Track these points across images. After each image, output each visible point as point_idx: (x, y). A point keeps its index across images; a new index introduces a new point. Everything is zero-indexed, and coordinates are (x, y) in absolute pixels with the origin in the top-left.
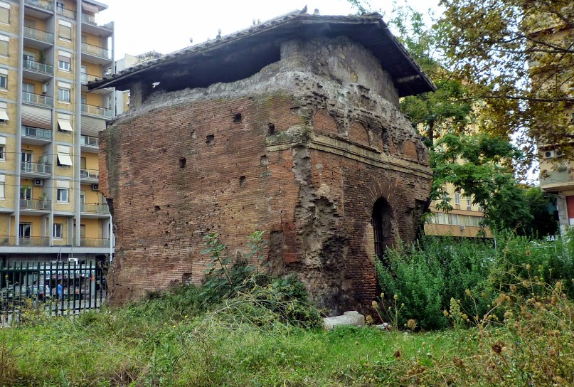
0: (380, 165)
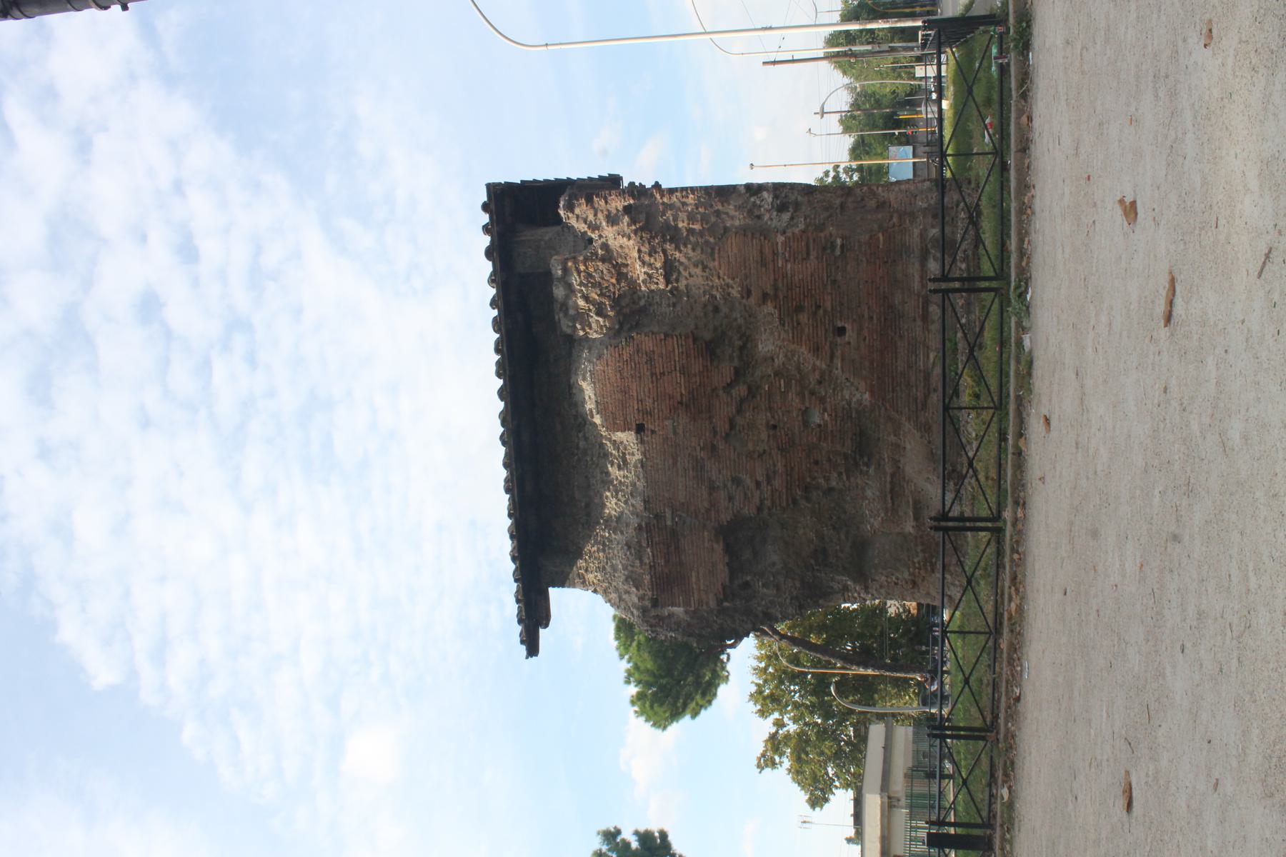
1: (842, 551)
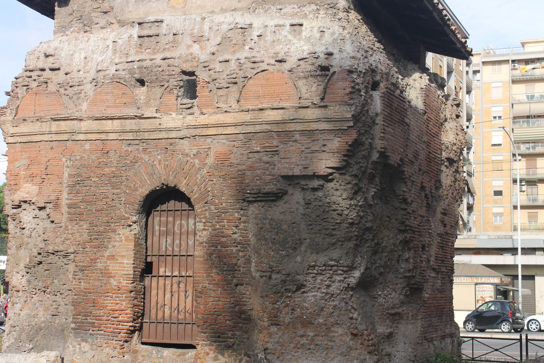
0: (163, 135)
1: (375, 269)
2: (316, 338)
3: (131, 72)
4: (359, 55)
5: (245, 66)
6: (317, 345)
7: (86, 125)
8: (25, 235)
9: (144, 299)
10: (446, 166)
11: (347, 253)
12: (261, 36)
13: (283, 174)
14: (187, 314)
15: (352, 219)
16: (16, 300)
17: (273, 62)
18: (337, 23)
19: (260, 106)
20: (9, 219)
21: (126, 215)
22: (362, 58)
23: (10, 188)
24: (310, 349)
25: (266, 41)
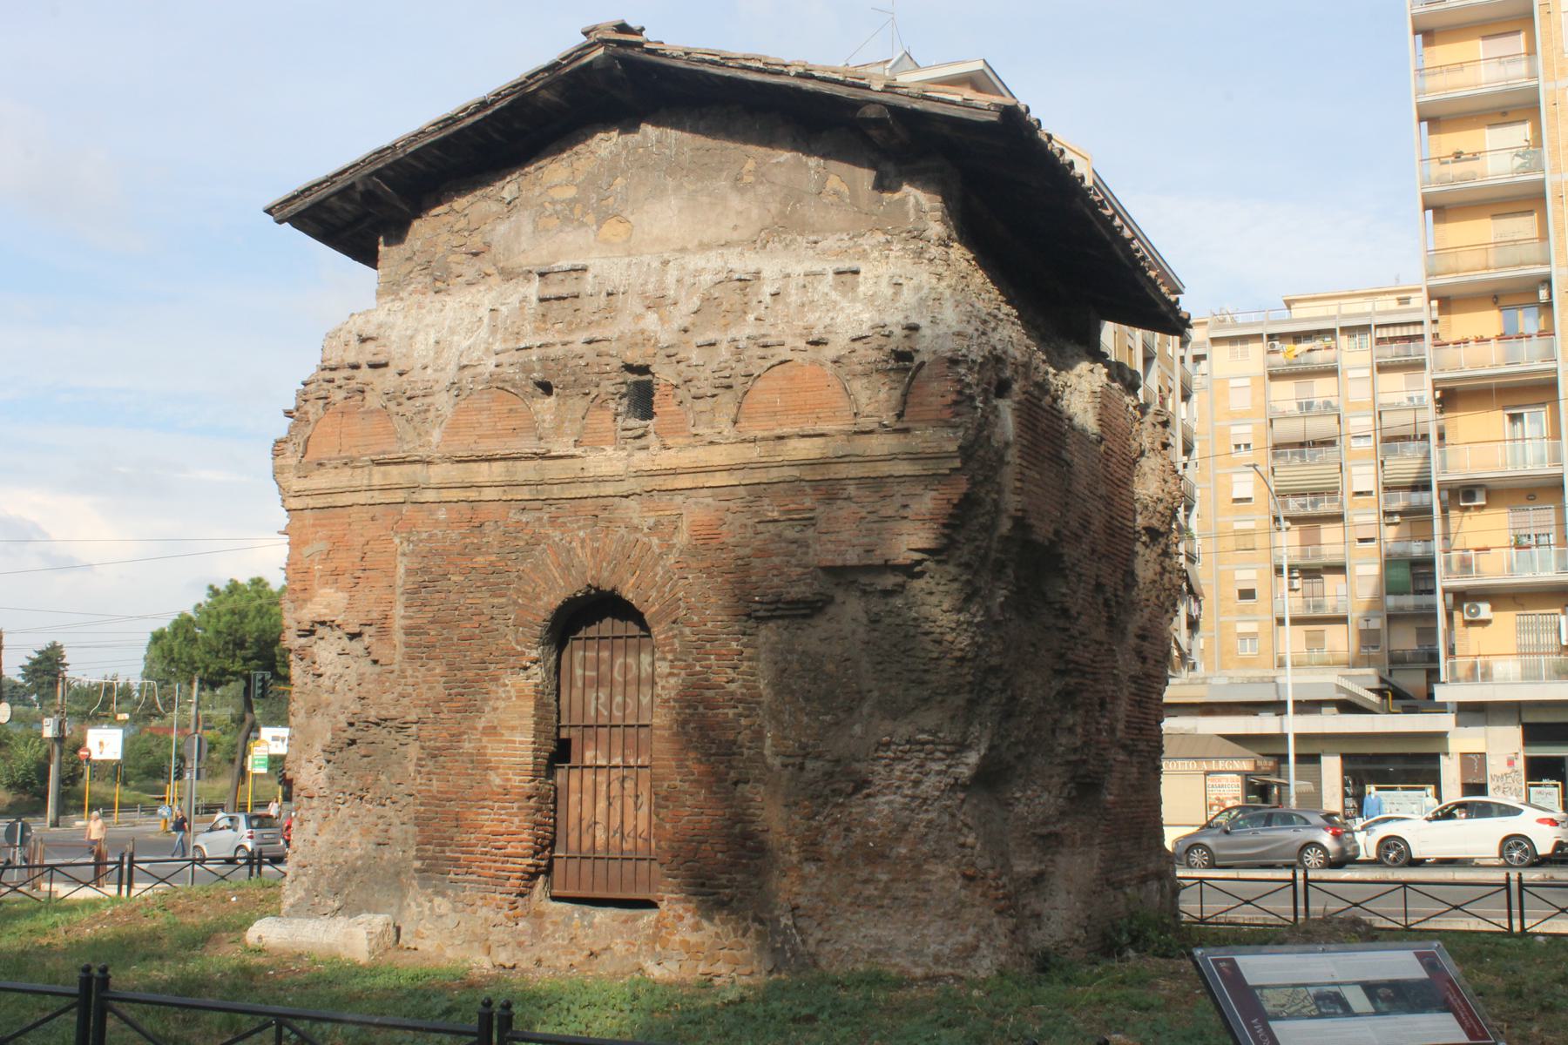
0: (590, 490)
1: (1008, 748)
2: (896, 885)
3: (526, 368)
4: (970, 330)
5: (748, 353)
6: (896, 899)
7: (438, 473)
8: (323, 688)
9: (555, 811)
10: (1144, 543)
11: (952, 718)
12: (778, 294)
13: (824, 563)
14: (640, 841)
15: (961, 650)
16: (308, 815)
17: (802, 344)
18: (925, 266)
19: (778, 432)
20: (292, 657)
21: (519, 648)
22: (976, 334)
23: (294, 597)
24: (882, 907)
25: (787, 305)
